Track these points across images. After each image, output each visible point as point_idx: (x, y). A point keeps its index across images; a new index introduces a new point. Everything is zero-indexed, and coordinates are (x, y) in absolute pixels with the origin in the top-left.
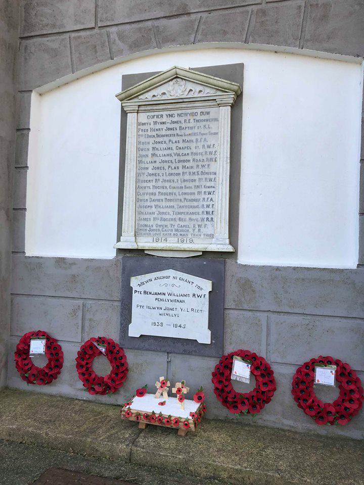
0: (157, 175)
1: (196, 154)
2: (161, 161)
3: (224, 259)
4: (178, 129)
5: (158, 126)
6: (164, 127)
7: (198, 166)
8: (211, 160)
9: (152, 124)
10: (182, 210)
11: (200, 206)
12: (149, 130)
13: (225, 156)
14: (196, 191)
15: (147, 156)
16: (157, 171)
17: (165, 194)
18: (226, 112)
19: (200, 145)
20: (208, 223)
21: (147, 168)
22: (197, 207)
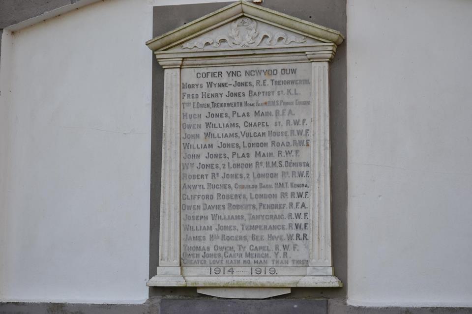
0: (214, 166)
1: (277, 134)
2: (220, 145)
3: (325, 299)
4: (247, 94)
5: (215, 90)
6: (224, 91)
7: (280, 153)
8: (301, 143)
9: (205, 85)
10: (255, 223)
11: (286, 215)
12: (200, 96)
13: (322, 139)
14: (278, 192)
15: (198, 136)
16: (214, 161)
17: (229, 197)
18: (320, 71)
19: (283, 120)
20: (299, 242)
21: (198, 156)
22: (281, 217)
